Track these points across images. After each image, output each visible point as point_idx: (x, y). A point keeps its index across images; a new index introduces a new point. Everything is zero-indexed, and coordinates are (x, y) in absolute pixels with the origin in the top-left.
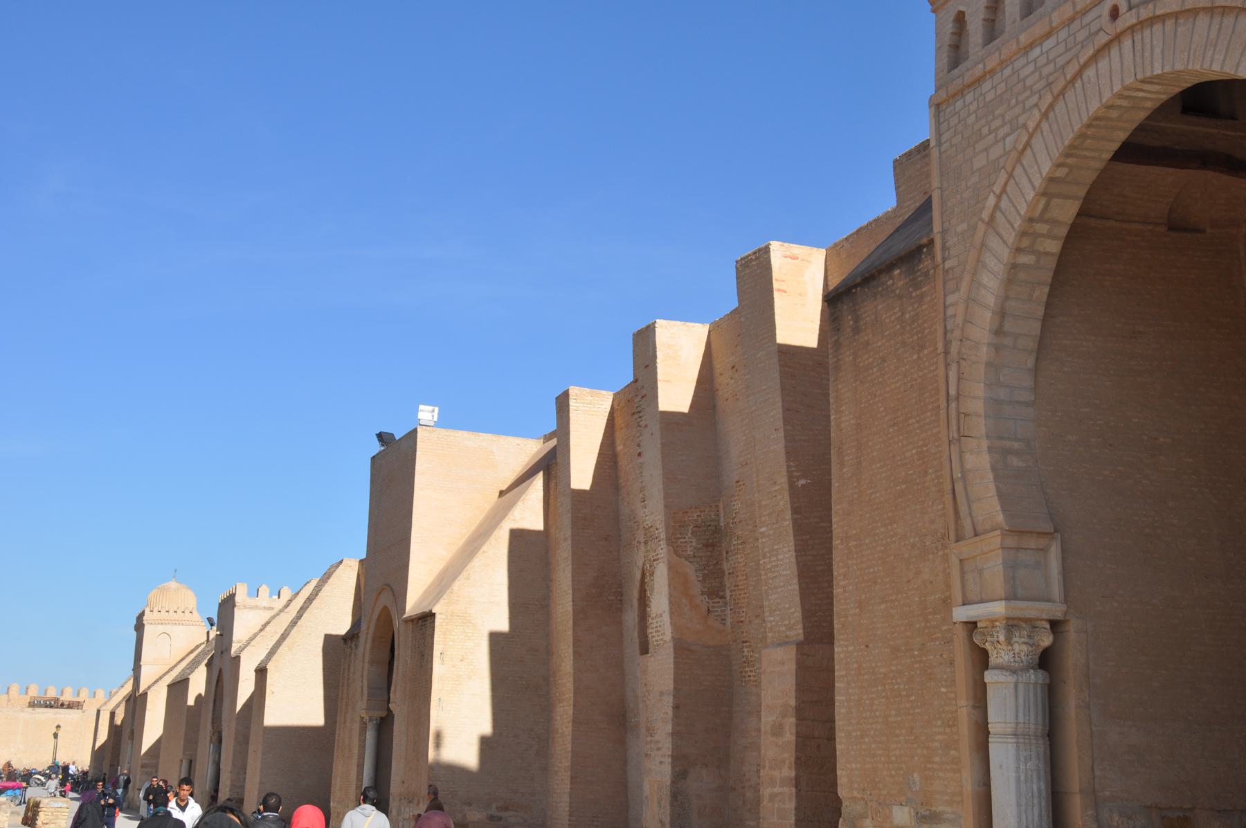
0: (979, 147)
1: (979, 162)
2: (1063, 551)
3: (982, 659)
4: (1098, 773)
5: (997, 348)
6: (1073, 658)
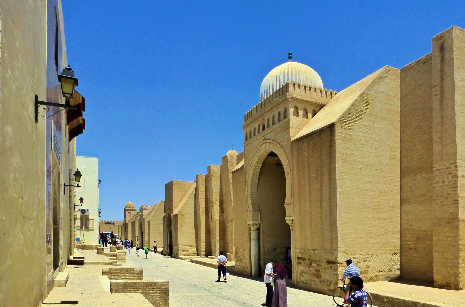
3: (250, 229)
5: (252, 185)
6: (262, 229)
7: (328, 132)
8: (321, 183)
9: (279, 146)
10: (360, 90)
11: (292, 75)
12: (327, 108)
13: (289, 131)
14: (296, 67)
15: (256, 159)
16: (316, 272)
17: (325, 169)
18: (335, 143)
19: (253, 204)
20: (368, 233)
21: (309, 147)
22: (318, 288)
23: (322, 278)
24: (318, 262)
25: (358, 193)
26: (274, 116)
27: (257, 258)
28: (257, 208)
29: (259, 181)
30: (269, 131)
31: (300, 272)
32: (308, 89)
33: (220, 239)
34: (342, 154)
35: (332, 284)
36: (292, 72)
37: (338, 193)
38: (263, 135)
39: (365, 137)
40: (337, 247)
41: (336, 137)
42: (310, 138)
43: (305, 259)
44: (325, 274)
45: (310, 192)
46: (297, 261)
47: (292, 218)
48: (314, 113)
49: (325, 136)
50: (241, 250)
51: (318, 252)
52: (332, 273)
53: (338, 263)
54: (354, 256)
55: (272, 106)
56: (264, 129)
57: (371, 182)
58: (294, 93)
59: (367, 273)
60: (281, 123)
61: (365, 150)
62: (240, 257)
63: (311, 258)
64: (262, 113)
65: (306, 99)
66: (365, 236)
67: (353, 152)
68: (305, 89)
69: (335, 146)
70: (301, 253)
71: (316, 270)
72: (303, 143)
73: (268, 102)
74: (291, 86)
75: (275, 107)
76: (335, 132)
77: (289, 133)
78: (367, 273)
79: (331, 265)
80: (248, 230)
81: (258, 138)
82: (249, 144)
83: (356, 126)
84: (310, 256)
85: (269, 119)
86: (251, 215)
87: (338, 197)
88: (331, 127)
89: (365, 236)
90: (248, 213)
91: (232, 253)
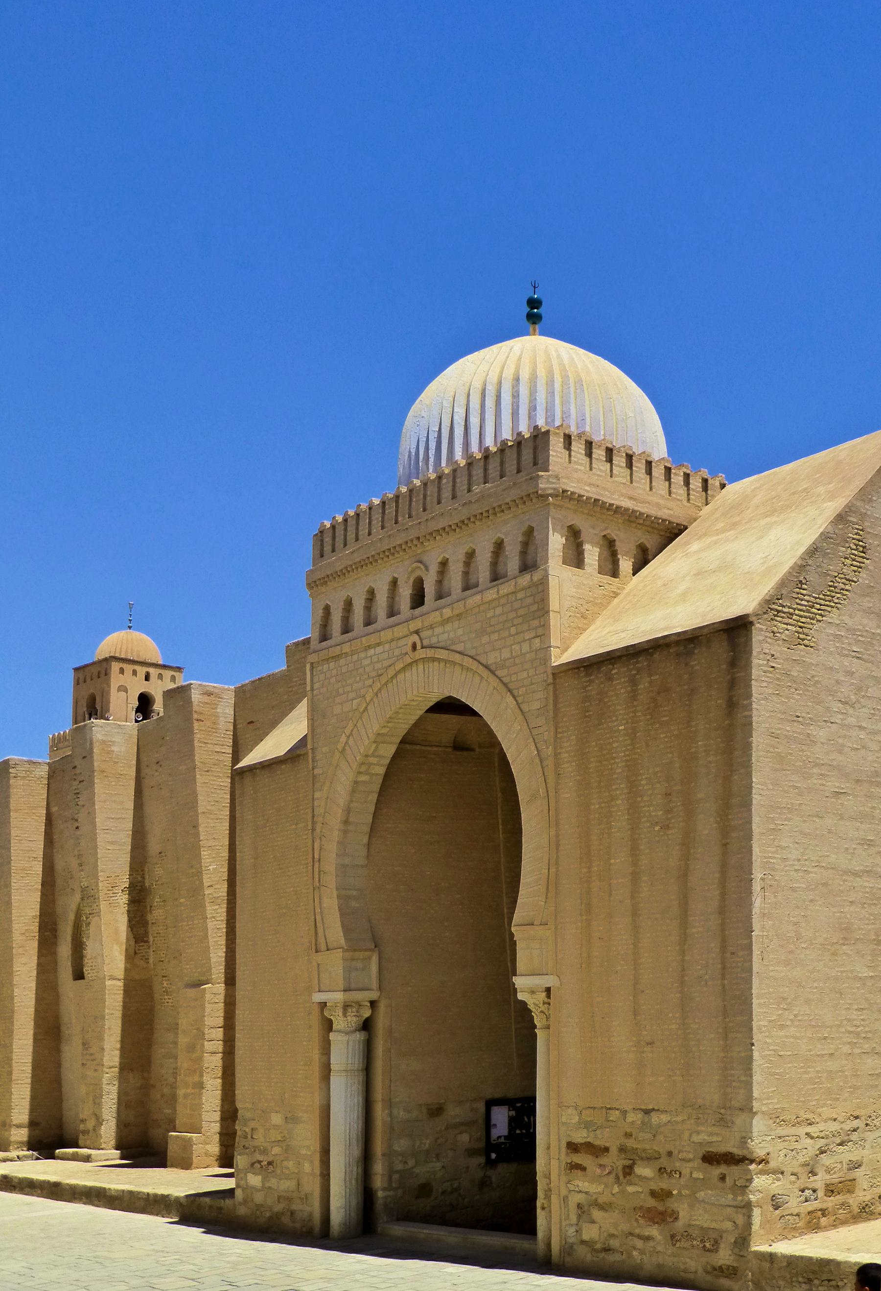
0: (338, 700)
1: (337, 710)
2: (380, 958)
3: (328, 1025)
4: (392, 1089)
5: (345, 832)
6: (382, 1023)
7: (720, 649)
8: (687, 843)
9: (492, 678)
10: (832, 496)
11: (551, 393)
12: (695, 546)
13: (546, 626)
14: (566, 361)
15: (373, 724)
16: (651, 1202)
17: (706, 792)
18: (749, 696)
19: (345, 913)
20: (858, 1034)
21: (633, 696)
22: (659, 1266)
23: (680, 1224)
24: (664, 1162)
25: (825, 884)
26: (471, 555)
27: (357, 1152)
28: (365, 935)
29: (375, 815)
30: (447, 612)
31: (579, 1206)
32: (619, 461)
33: (124, 1068)
34: (772, 735)
35: (722, 1245)
36: (550, 382)
37: (756, 887)
38: (415, 625)
39: (851, 674)
40: (750, 1097)
41: (755, 673)
42: (643, 662)
43: (606, 1150)
44: (691, 1206)
45: (635, 877)
46: (566, 1158)
47: (549, 981)
48: (642, 560)
49: (709, 663)
50: (276, 1119)
51: (664, 1118)
52: (723, 1201)
53: (752, 1161)
54: (809, 1129)
55: (464, 513)
56: (418, 599)
57: (870, 843)
58: (566, 471)
59: (851, 1191)
60: (506, 588)
61: (851, 720)
62: (264, 1152)
63: (631, 1143)
64: (413, 533)
65: (616, 503)
66: (846, 1049)
67: (813, 730)
68: (610, 459)
69: (749, 707)
70: (587, 1125)
71: (653, 1194)
72: (610, 679)
73: (446, 494)
74: (556, 445)
75: (481, 516)
76: (750, 653)
77: (543, 631)
78: (851, 1191)
79: (723, 1169)
80: (315, 1032)
81: (386, 635)
82: (337, 658)
83: (821, 632)
84: (628, 1135)
85: (444, 564)
86: (334, 964)
87: (758, 903)
88: (737, 629)
89: (846, 1049)
90: (319, 958)
91: (196, 1129)
